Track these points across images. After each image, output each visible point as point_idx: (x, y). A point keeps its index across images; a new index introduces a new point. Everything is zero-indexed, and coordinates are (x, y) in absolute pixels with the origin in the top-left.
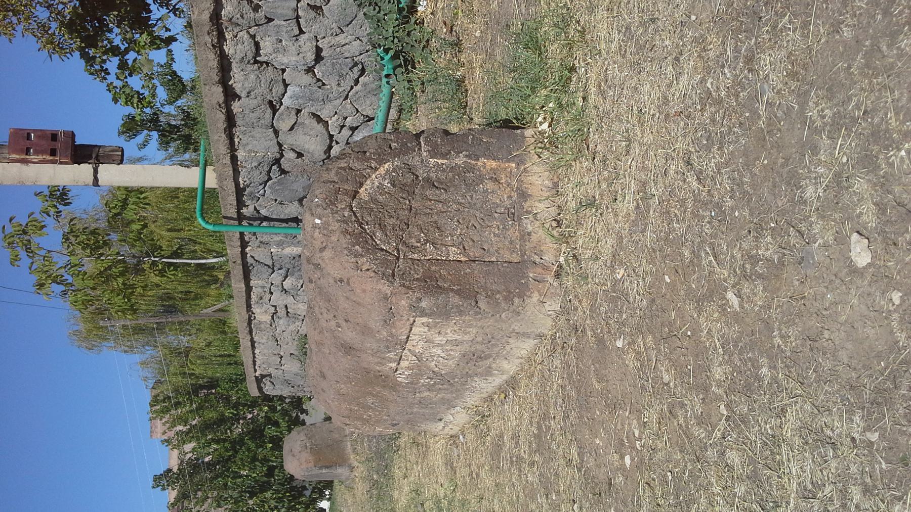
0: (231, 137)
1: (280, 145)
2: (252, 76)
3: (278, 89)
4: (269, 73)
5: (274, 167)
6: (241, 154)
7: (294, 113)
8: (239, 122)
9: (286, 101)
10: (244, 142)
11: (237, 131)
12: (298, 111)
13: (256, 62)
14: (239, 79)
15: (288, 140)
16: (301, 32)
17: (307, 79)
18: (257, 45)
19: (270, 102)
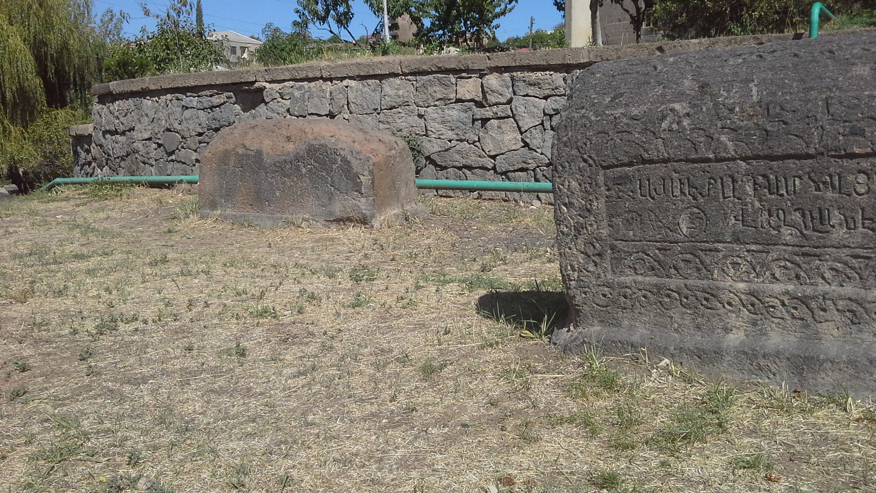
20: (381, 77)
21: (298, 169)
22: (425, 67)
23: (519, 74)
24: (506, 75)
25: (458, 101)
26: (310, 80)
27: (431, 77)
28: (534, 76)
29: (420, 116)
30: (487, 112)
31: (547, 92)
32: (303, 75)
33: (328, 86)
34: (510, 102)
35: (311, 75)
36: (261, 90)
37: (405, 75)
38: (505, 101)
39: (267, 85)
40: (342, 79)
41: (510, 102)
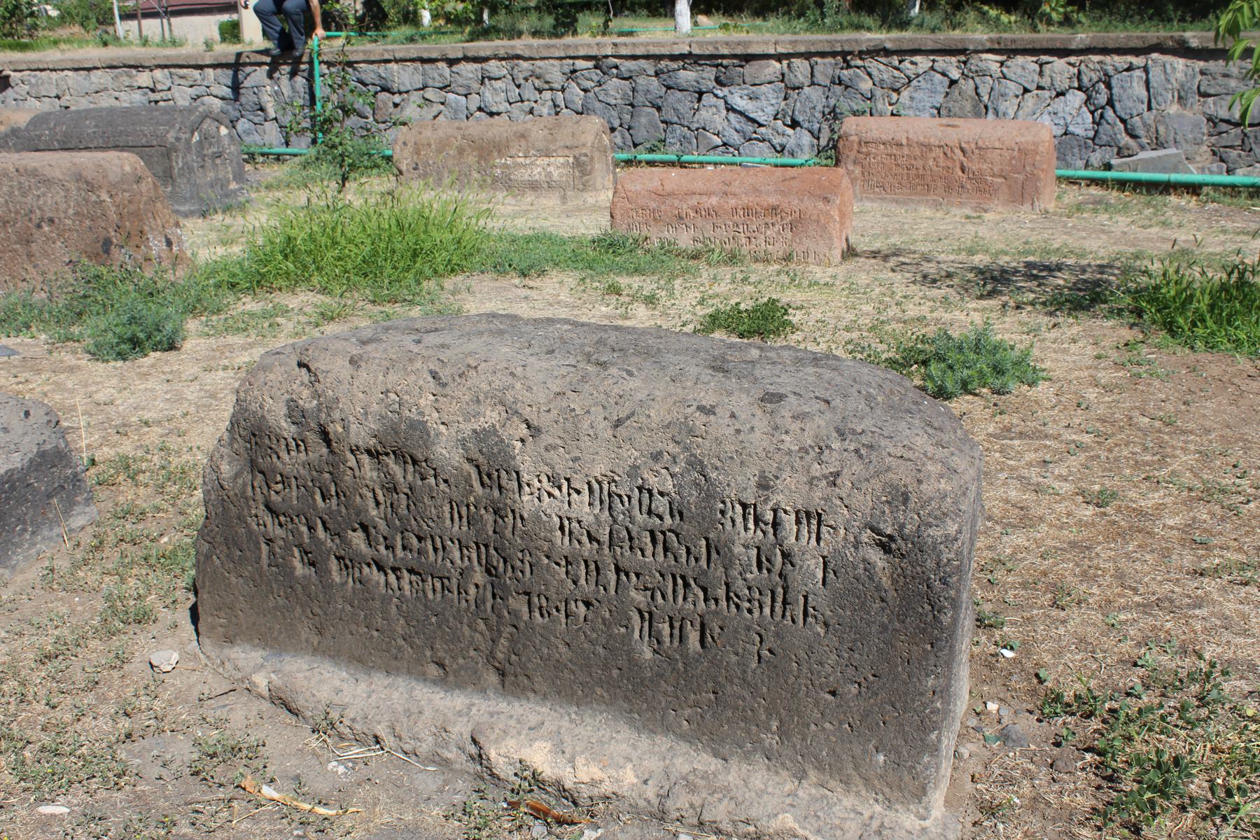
0: (413, 60)
1: (407, 92)
2: (471, 76)
3: (462, 91)
4: (476, 86)
5: (379, 88)
6: (393, 66)
7: (442, 100)
8: (427, 66)
9: (451, 96)
10: (407, 68)
11: (418, 65)
12: (442, 104)
13: (483, 78)
14: (467, 69)
15: (415, 97)
16: (510, 104)
17: (473, 108)
18: (499, 79)
19: (449, 86)
20: (89, 70)
21: (7, 143)
22: (115, 64)
23: (172, 70)
24: (166, 70)
25: (139, 88)
26: (42, 70)
27: (120, 70)
28: (185, 71)
29: (117, 99)
30: (157, 96)
31: (192, 83)
32: (35, 67)
33: (54, 75)
34: (169, 89)
35: (41, 67)
36: (8, 77)
37: (103, 68)
38: (166, 88)
39: (12, 74)
40: (63, 70)
41: (169, 89)
